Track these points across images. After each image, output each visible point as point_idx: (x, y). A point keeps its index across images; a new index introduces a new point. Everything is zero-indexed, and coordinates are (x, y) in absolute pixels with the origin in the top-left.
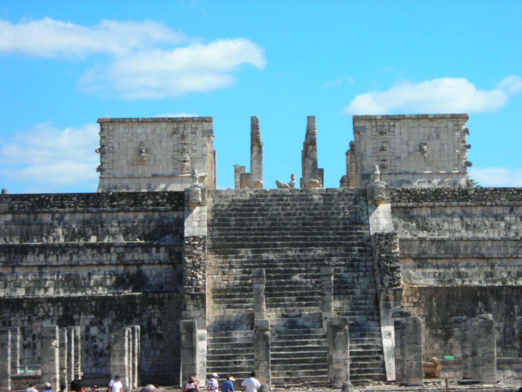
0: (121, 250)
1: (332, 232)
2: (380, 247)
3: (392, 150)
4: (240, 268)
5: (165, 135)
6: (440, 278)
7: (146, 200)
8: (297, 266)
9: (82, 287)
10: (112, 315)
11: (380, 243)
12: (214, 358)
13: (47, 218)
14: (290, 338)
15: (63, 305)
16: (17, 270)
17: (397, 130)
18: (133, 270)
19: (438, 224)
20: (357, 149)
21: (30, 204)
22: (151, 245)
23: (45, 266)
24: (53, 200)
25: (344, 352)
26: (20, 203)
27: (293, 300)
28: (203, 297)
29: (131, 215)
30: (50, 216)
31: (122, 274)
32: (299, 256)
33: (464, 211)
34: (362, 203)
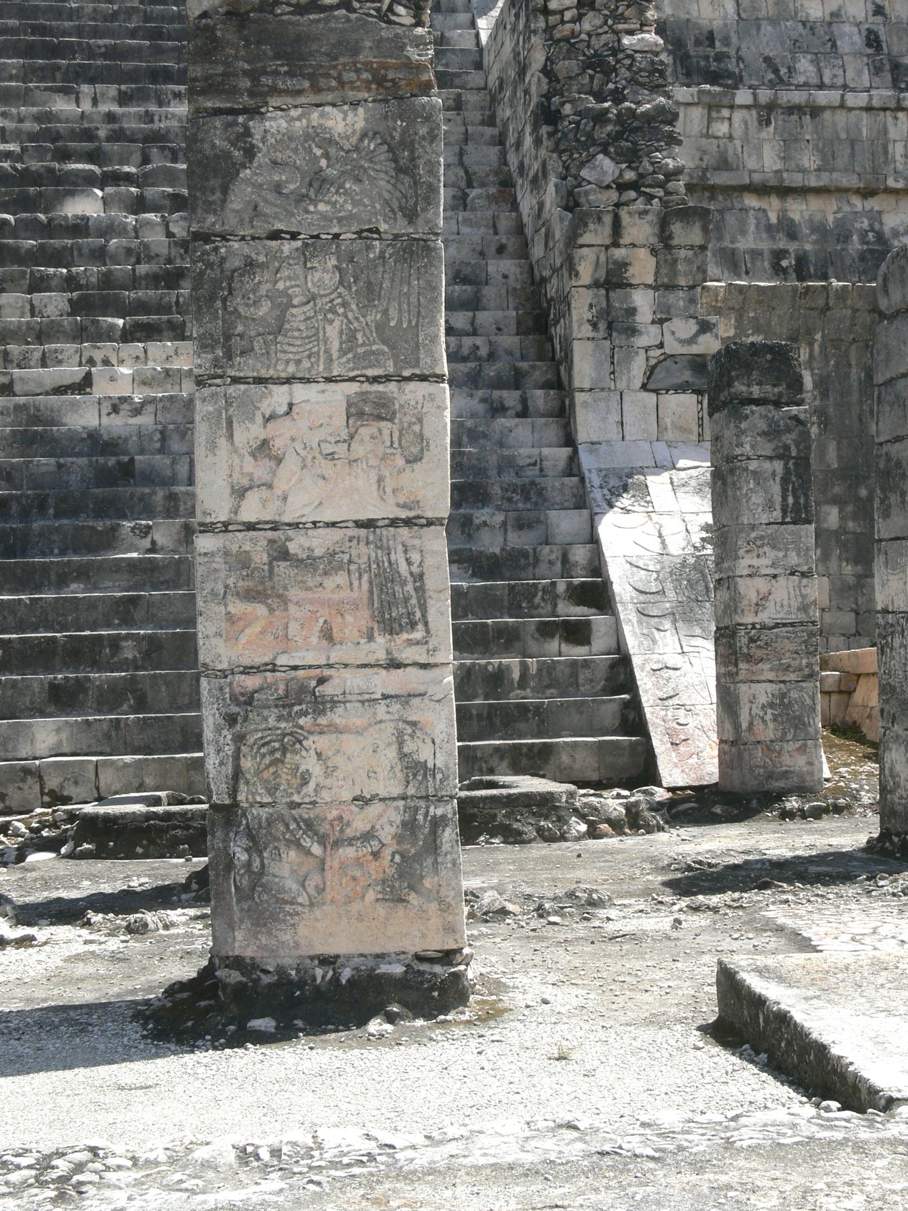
2: (549, 29)
19: (767, 60)
25: (367, 411)
32: (111, 117)
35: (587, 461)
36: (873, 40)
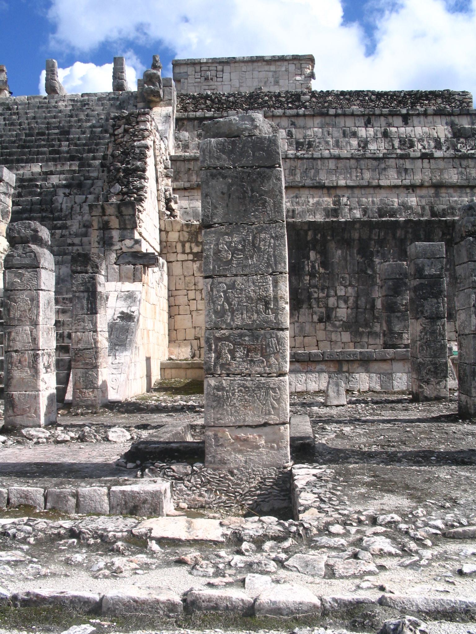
2: (115, 140)
11: (116, 133)
17: (226, 76)
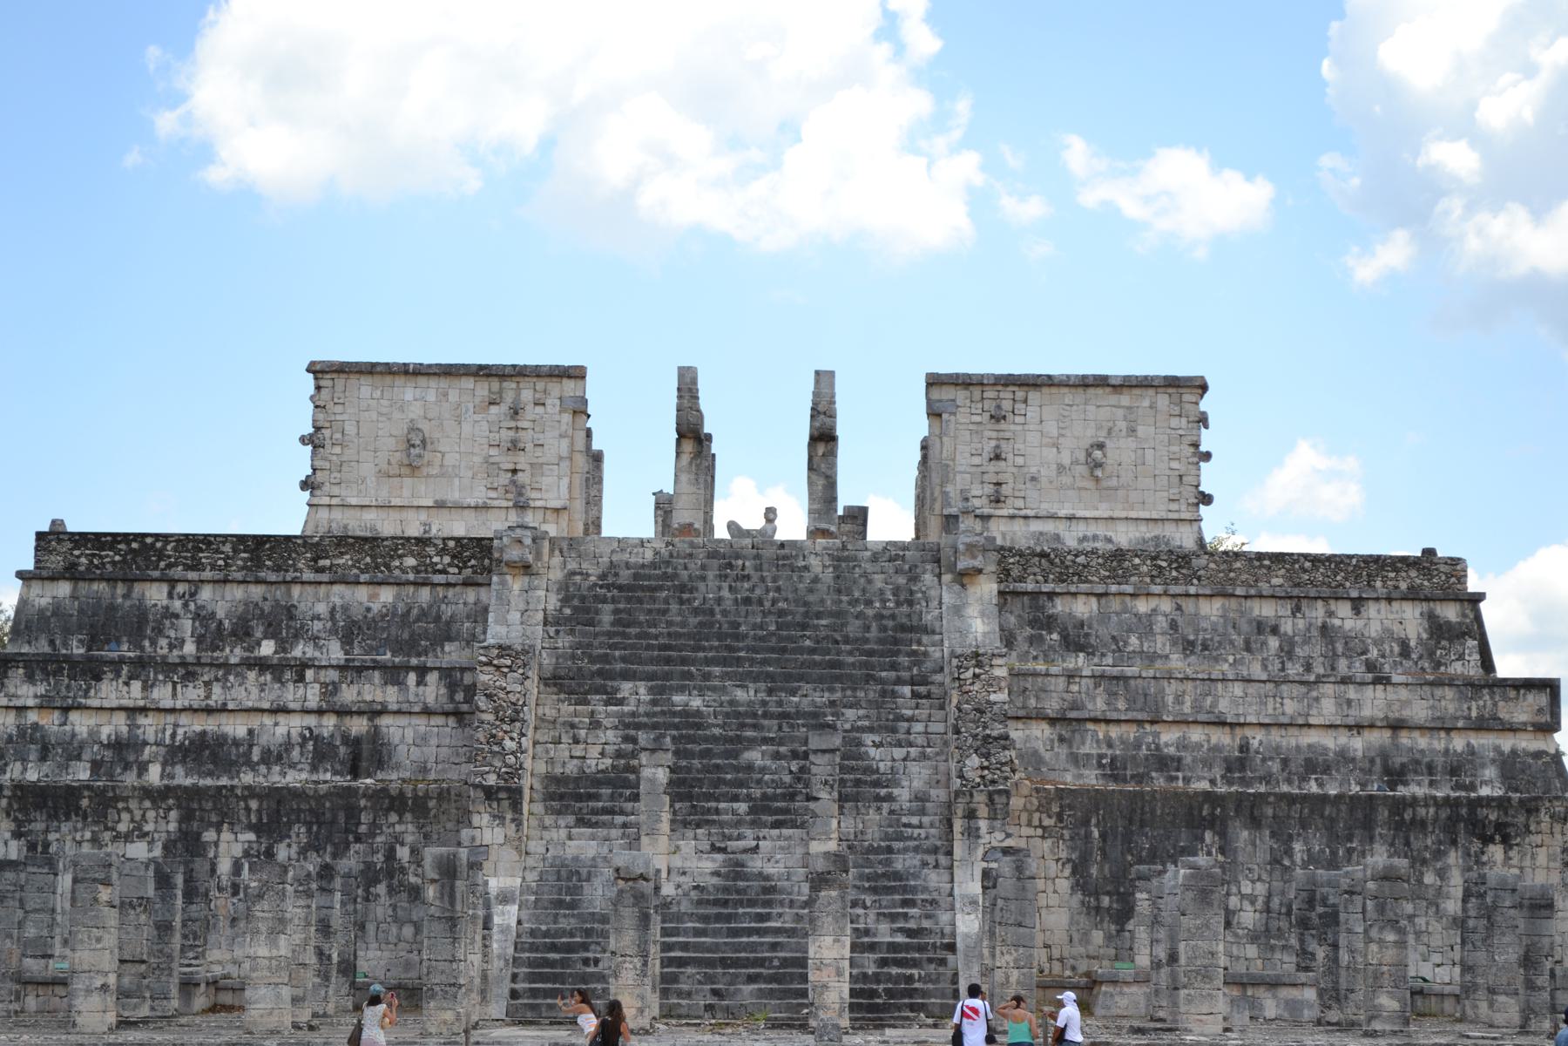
0: (333, 675)
1: (848, 647)
3: (1020, 461)
4: (616, 728)
5: (471, 406)
6: (1114, 769)
7: (400, 557)
8: (755, 727)
9: (233, 763)
10: (298, 835)
12: (533, 948)
13: (156, 594)
14: (725, 903)
15: (179, 807)
16: (74, 716)
17: (1033, 412)
18: (358, 726)
19: (1113, 638)
20: (934, 453)
21: (117, 558)
22: (408, 668)
23: (144, 710)
24: (175, 549)
26: (94, 555)
27: (741, 811)
28: (515, 796)
29: (362, 593)
30: (165, 588)
31: (332, 736)
32: (764, 703)
33: (1179, 608)
34: (928, 578)
35: (956, 892)
36: (1173, 625)
